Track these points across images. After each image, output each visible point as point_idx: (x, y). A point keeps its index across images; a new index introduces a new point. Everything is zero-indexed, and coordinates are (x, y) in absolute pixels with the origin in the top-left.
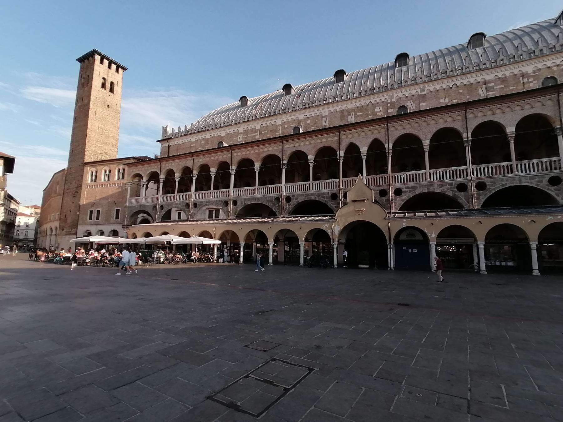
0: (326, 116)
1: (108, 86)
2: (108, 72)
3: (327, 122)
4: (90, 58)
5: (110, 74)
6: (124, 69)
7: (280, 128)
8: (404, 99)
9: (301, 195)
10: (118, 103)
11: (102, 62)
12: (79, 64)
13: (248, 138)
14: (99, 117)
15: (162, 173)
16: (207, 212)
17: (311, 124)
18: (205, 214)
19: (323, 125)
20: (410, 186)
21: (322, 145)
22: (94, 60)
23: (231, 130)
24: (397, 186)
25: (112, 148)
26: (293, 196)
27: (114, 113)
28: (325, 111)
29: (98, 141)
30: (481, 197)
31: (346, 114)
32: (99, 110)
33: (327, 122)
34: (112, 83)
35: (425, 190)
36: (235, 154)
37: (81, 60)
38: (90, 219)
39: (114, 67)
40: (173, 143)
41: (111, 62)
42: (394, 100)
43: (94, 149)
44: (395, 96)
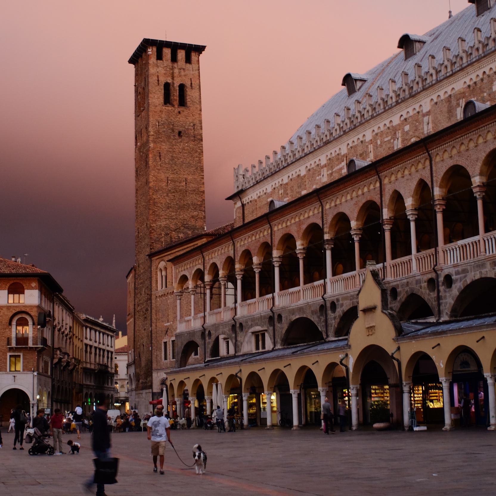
0: (428, 113)
1: (175, 95)
2: (173, 69)
3: (431, 125)
4: (144, 55)
5: (176, 71)
6: (200, 49)
7: (371, 147)
9: (345, 298)
11: (159, 57)
12: (132, 66)
13: (334, 174)
15: (206, 272)
16: (253, 340)
17: (411, 133)
18: (251, 342)
19: (426, 132)
20: (460, 269)
21: (364, 201)
22: (148, 56)
23: (311, 162)
24: (446, 272)
25: (195, 213)
26: (338, 300)
27: (191, 145)
28: (425, 103)
29: (168, 208)
31: (454, 103)
32: (165, 147)
34: (182, 87)
35: (478, 277)
36: (276, 229)
38: (166, 358)
39: (181, 54)
40: (247, 198)
41: (175, 47)
43: (163, 223)
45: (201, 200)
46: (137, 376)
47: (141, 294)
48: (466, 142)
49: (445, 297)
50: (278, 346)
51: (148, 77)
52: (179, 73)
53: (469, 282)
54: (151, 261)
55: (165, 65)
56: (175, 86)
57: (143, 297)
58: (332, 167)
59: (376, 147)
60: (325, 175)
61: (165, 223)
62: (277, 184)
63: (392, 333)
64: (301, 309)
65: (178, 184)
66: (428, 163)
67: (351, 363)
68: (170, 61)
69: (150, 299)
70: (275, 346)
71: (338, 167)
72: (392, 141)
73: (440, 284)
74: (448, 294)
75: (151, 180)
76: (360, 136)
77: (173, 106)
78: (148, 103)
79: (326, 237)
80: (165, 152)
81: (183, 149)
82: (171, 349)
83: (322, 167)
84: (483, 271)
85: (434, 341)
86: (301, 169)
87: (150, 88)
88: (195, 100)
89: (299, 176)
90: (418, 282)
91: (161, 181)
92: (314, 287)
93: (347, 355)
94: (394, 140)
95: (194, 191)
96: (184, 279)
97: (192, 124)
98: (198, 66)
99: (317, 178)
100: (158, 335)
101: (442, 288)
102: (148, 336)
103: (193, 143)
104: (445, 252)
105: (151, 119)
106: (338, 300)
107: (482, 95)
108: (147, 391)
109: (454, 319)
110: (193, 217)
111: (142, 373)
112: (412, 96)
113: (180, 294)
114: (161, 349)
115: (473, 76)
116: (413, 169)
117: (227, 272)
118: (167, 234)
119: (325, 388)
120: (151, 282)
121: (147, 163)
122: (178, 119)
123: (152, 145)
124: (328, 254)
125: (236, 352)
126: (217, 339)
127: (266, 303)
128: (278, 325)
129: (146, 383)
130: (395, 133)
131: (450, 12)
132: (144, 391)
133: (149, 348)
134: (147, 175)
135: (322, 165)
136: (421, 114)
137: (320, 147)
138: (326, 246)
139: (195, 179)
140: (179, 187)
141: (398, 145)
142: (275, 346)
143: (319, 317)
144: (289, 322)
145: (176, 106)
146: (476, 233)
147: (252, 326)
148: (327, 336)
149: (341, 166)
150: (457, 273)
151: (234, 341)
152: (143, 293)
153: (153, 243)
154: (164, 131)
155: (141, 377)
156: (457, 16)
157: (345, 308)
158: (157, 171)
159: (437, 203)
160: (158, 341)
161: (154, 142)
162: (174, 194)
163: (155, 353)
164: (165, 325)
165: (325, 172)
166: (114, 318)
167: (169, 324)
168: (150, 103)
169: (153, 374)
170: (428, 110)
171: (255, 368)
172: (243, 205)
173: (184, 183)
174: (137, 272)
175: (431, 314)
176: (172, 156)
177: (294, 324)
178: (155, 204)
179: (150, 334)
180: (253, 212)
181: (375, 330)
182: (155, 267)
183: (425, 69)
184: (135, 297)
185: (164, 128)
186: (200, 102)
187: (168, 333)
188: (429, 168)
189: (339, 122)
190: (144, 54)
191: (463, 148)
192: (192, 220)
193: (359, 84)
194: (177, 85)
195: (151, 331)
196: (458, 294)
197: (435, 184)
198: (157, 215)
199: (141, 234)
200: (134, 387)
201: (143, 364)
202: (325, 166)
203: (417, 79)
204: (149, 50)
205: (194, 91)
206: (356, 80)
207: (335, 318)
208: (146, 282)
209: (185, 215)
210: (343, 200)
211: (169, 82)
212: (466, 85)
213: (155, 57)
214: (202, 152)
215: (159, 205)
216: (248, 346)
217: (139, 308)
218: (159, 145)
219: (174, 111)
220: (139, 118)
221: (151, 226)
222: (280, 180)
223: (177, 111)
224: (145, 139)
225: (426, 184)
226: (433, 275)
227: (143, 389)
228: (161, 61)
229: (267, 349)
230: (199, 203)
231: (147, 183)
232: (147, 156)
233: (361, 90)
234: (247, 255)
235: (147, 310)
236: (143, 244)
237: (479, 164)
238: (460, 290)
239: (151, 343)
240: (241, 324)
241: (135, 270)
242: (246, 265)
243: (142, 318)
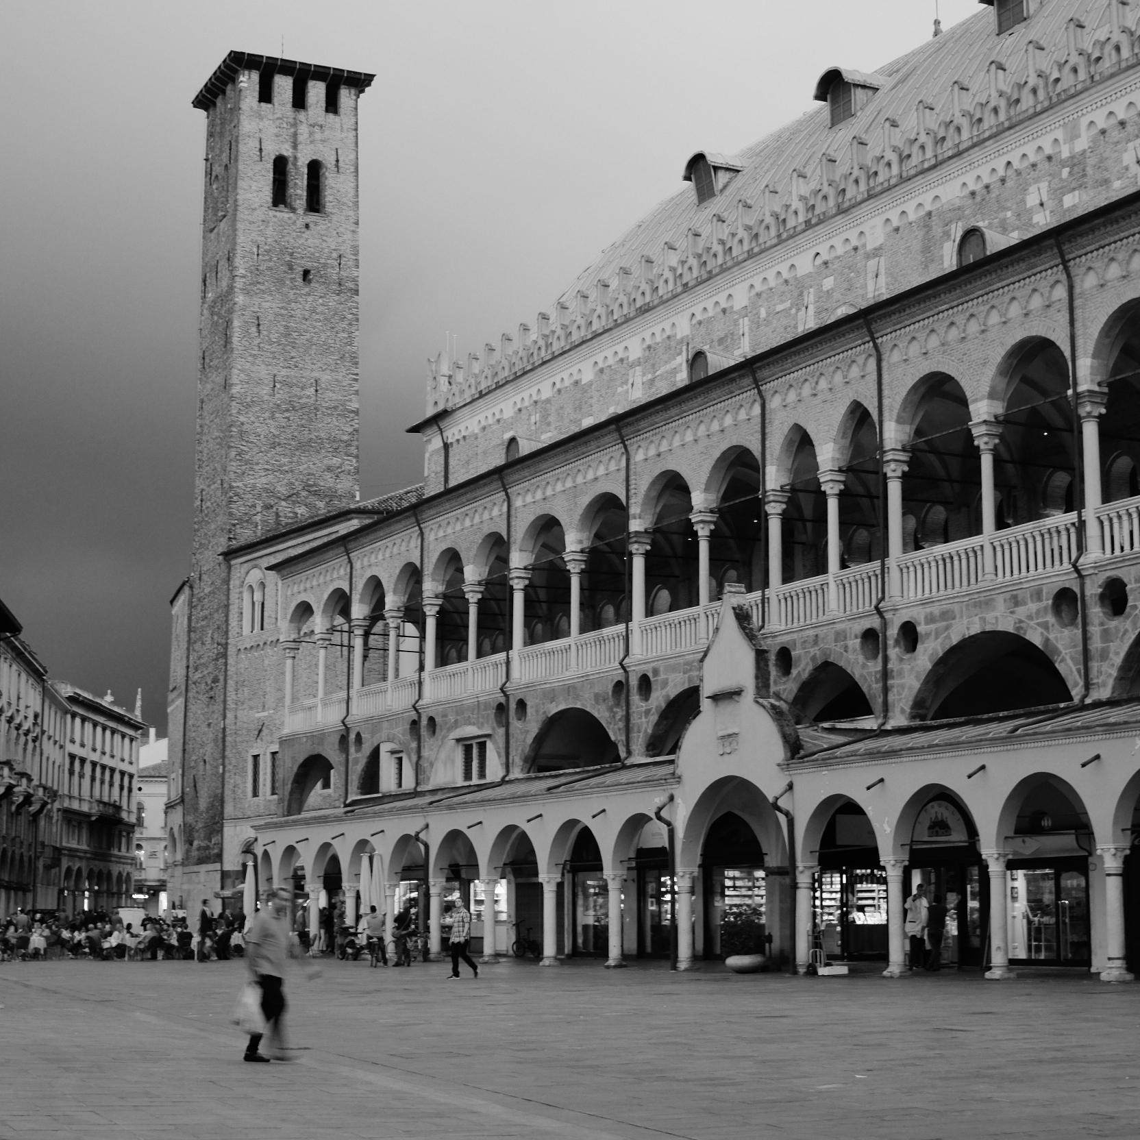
0: (877, 252)
3: (882, 279)
5: (303, 130)
6: (360, 82)
7: (745, 324)
8: (1115, 135)
10: (346, 249)
11: (266, 95)
12: (202, 113)
13: (658, 384)
14: (274, 337)
15: (356, 598)
18: (453, 762)
20: (936, 610)
21: (724, 446)
23: (606, 353)
24: (904, 616)
25: (336, 461)
26: (656, 672)
27: (333, 301)
28: (872, 227)
29: (273, 446)
30: (1113, 646)
31: (937, 230)
32: (269, 305)
33: (882, 279)
34: (315, 168)
35: (975, 629)
37: (207, 99)
38: (255, 794)
39: (316, 91)
40: (455, 430)
41: (302, 74)
42: (1082, 144)
43: (261, 482)
44: (1084, 122)
45: (350, 430)
46: (189, 833)
47: (203, 644)
48: (960, 319)
49: (900, 673)
50: (516, 773)
51: (237, 141)
52: (311, 134)
53: (955, 640)
54: (229, 567)
55: (279, 115)
56: (300, 163)
57: (208, 650)
58: (653, 365)
59: (756, 324)
60: (638, 385)
61: (264, 480)
62: (526, 399)
63: (778, 751)
64: (570, 690)
65: (296, 391)
66: (872, 363)
67: (681, 815)
68: (290, 105)
69: (225, 656)
70: (508, 771)
71: (668, 367)
72: (793, 311)
73: (891, 642)
74: (906, 667)
75: (235, 380)
76: (722, 298)
77: (293, 210)
78: (236, 201)
79: (635, 525)
80: (271, 317)
81: (314, 311)
82: (269, 771)
83: (632, 366)
84: (990, 616)
85: (872, 771)
86: (583, 368)
87: (240, 167)
88: (344, 200)
89: (576, 382)
90: (840, 636)
91: (259, 382)
92: (601, 641)
93: (672, 798)
94: (799, 310)
95: (335, 408)
96: (305, 610)
97: (335, 255)
98: (353, 120)
99: (620, 389)
100: (238, 739)
101: (894, 652)
102: (215, 740)
103: (337, 298)
104: (905, 570)
105: (241, 239)
106: (656, 672)
107: (1001, 215)
108: (211, 867)
109: (918, 722)
110: (329, 469)
111: (200, 825)
112: (842, 211)
113: (293, 645)
114: (244, 771)
115: (984, 172)
116: (838, 378)
117: (404, 599)
118: (268, 507)
119: (620, 872)
120: (227, 616)
121: (227, 340)
122: (302, 241)
123: (240, 299)
124: (638, 565)
125: (417, 784)
126: (375, 754)
127: (490, 672)
128: (515, 724)
129: (208, 848)
130: (801, 294)
131: (937, 23)
132: (203, 868)
133: (217, 767)
134: (227, 367)
135: (631, 359)
136: (861, 252)
137: (627, 320)
138: (634, 548)
139: (337, 380)
140: (300, 398)
141: (808, 322)
142: (508, 771)
143: (611, 709)
144: (541, 718)
145: (301, 211)
146: (976, 529)
147: (456, 725)
148: (629, 753)
149: (674, 364)
150: (930, 619)
151: (414, 758)
152: (208, 640)
153: (234, 525)
154: (270, 269)
155: (196, 835)
156: (953, 31)
157: (673, 691)
158: (250, 359)
159: (889, 456)
160: (239, 753)
161: (247, 292)
162: (287, 415)
163: (230, 782)
164: (257, 715)
165: (638, 377)
166: (139, 697)
167: (265, 714)
168: (240, 203)
169: (226, 829)
170: (877, 245)
171: (459, 821)
172: (446, 446)
173: (312, 390)
174: (196, 591)
175: (867, 710)
176: (286, 327)
177: (553, 724)
178: (242, 433)
179: (221, 735)
180: (468, 462)
181: (739, 743)
182: (238, 582)
183: (874, 150)
184: (188, 649)
185: (270, 260)
186: (356, 204)
187: (263, 734)
188: (874, 376)
189: (674, 263)
190: (229, 87)
191: (954, 333)
192: (328, 475)
193: (722, 178)
194: (303, 162)
195: (224, 729)
196: (929, 666)
197: (886, 414)
198: (247, 462)
199: (209, 504)
200: (179, 857)
201: (203, 804)
202: (638, 362)
203: (856, 172)
204: (241, 78)
205: (342, 177)
206: (716, 168)
207: (647, 712)
208: (216, 616)
209: (312, 464)
210: (677, 442)
211: (286, 154)
212: (966, 192)
213: (256, 94)
214: (357, 320)
215: (252, 438)
216: (446, 769)
217: (198, 675)
218: (256, 300)
219: (294, 223)
220: (213, 235)
221: (231, 487)
222: (534, 391)
223: (300, 223)
224: (224, 284)
225: (865, 414)
226: (875, 622)
227: (201, 861)
228: (269, 106)
229: (488, 780)
230: (345, 438)
231: (226, 385)
232: (228, 324)
233: (727, 192)
234: (452, 559)
235: (215, 680)
236: (213, 526)
237: (990, 371)
238: (936, 659)
239: (224, 757)
240: (431, 720)
241: (191, 587)
242: (449, 584)
243: (204, 698)
